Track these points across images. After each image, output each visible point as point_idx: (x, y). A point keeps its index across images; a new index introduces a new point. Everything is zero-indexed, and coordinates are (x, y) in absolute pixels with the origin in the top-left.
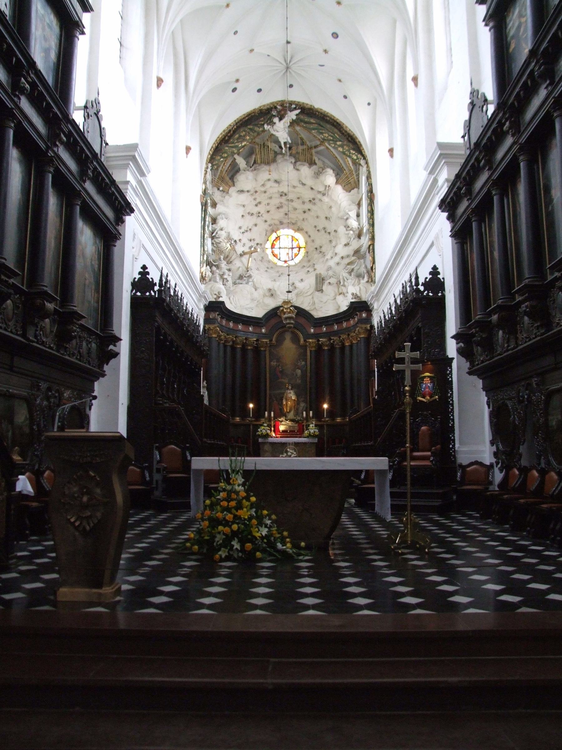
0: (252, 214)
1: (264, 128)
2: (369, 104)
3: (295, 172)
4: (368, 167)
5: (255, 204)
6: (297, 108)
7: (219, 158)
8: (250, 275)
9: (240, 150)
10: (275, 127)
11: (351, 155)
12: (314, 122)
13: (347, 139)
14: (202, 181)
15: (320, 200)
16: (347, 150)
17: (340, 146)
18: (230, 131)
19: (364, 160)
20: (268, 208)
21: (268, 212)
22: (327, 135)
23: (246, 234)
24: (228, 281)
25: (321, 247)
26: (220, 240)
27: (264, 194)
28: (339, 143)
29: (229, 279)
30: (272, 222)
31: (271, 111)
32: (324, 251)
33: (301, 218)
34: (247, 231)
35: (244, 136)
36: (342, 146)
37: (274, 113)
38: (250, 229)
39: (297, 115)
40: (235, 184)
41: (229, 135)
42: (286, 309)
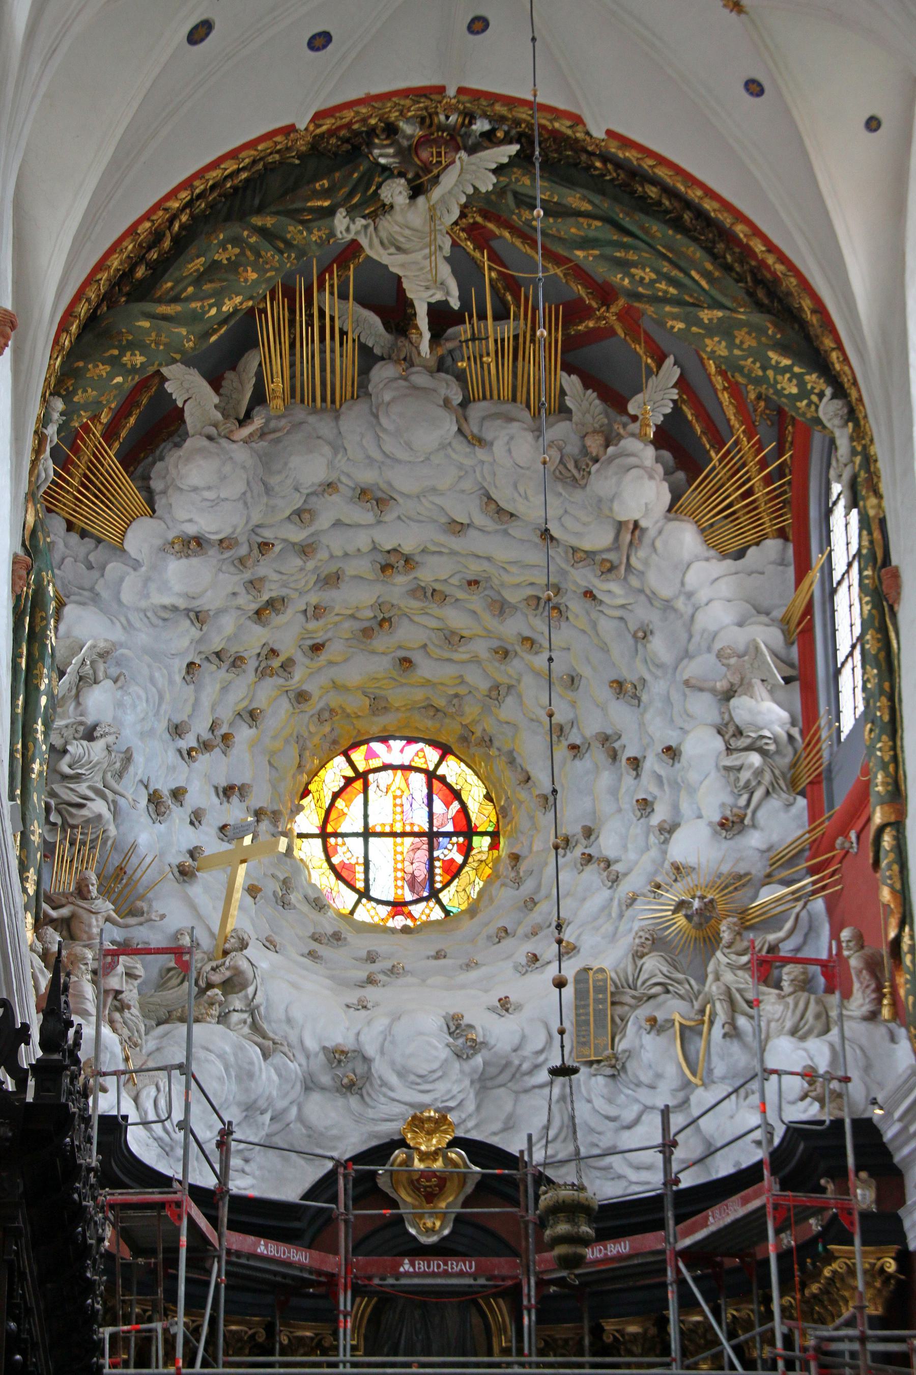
0: (237, 662)
1: (332, 234)
2: (873, 124)
3: (461, 450)
4: (860, 434)
5: (254, 606)
6: (500, 134)
7: (103, 370)
8: (237, 972)
9: (207, 334)
10: (387, 225)
11: (770, 373)
12: (586, 207)
13: (751, 294)
14: (24, 487)
15: (589, 594)
16: (751, 352)
17: (711, 330)
18: (157, 237)
19: (838, 403)
20: (318, 629)
21: (317, 648)
22: (649, 275)
23: (204, 760)
24: (122, 1007)
25: (588, 832)
26: (83, 788)
27: (298, 562)
28: (706, 315)
29: (131, 994)
30: (334, 699)
31: (370, 145)
32: (610, 853)
33: (484, 686)
34: (206, 746)
35: (234, 266)
36: (725, 330)
37: (384, 156)
38: (226, 738)
39: (499, 170)
40: (160, 503)
41: (154, 255)
42: (424, 1156)
